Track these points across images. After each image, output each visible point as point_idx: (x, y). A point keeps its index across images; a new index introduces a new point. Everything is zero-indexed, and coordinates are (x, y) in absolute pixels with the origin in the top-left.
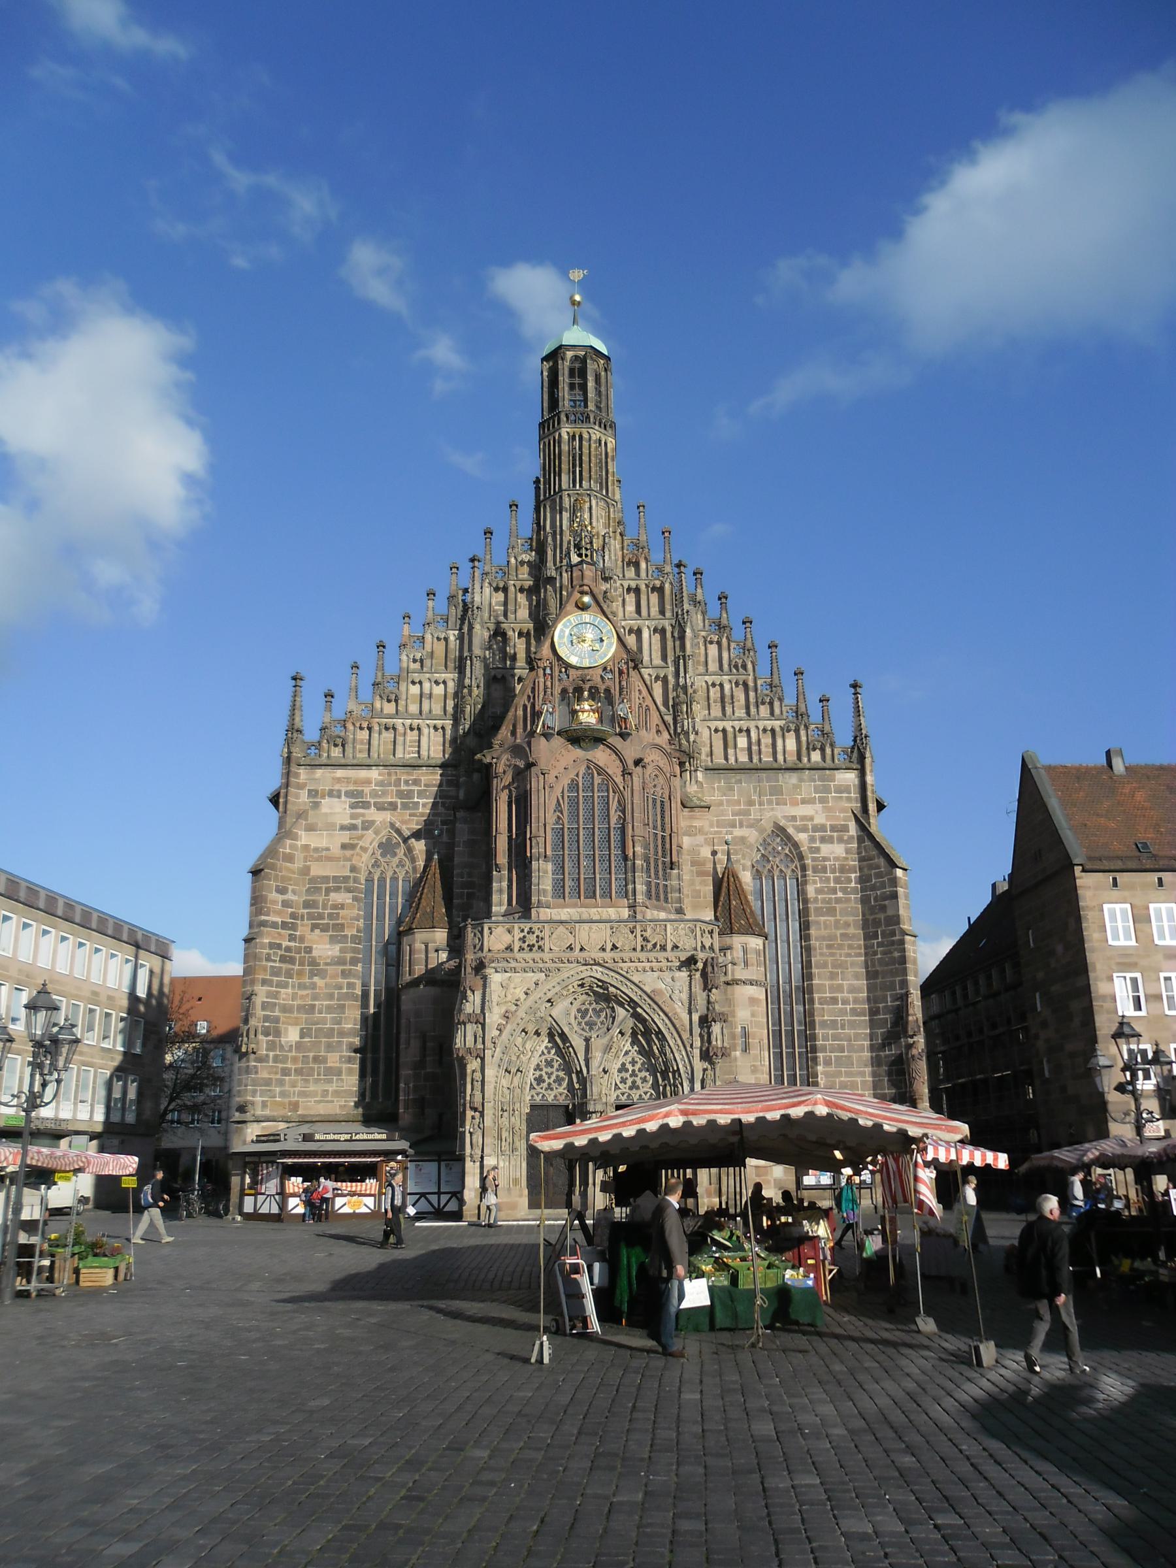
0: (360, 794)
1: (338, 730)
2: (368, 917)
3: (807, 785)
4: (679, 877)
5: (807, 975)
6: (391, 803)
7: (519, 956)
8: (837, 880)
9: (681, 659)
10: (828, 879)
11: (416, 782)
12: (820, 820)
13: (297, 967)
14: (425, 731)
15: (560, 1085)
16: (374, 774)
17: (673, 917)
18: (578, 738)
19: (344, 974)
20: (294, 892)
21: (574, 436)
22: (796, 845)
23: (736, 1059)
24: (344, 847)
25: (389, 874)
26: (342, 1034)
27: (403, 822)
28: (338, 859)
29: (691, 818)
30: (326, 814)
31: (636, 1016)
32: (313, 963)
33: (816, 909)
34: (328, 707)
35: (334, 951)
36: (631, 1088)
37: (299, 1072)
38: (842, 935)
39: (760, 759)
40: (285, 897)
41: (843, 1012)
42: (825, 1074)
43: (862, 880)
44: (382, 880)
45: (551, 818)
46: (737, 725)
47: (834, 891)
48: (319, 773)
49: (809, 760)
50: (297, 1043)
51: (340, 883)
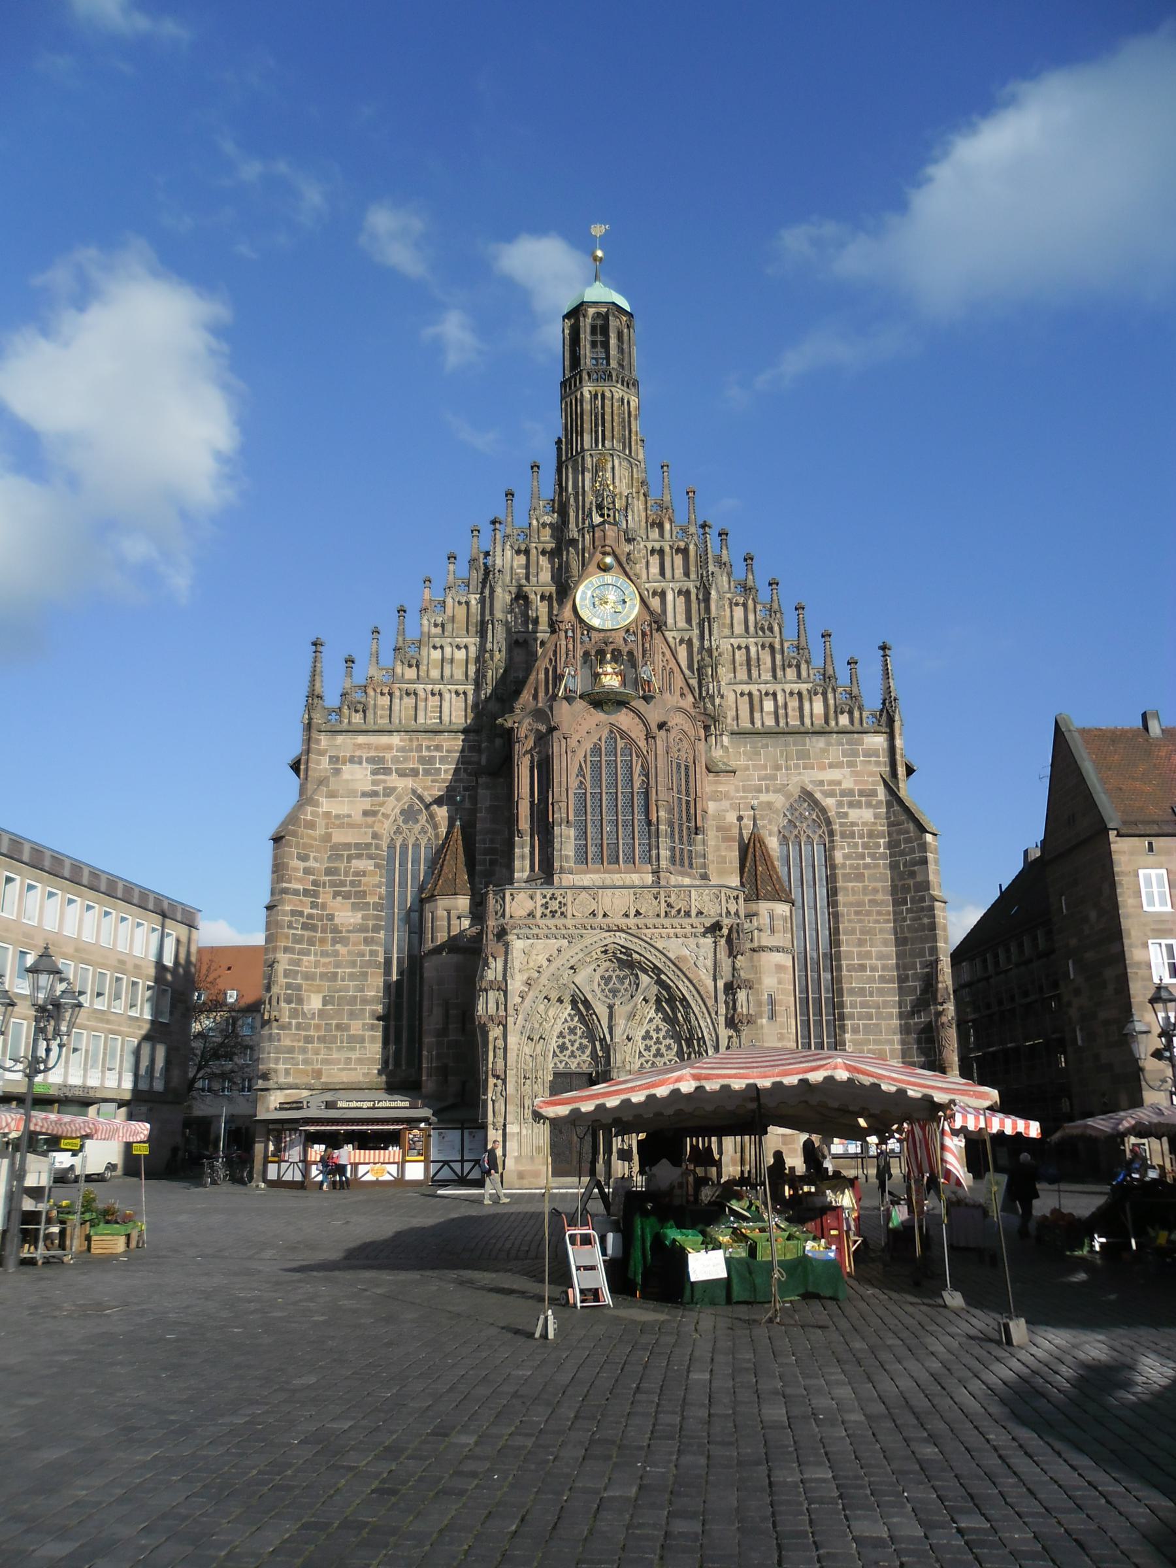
0: (382, 760)
1: (358, 696)
2: (390, 884)
3: (835, 749)
4: (704, 842)
5: (834, 942)
6: (412, 769)
7: (541, 922)
8: (865, 846)
9: (706, 622)
10: (856, 845)
11: (438, 748)
12: (848, 784)
13: (319, 935)
14: (447, 696)
15: (583, 1052)
16: (396, 740)
17: (698, 882)
18: (600, 701)
19: (367, 941)
20: (316, 859)
21: (596, 395)
22: (823, 810)
23: (762, 1026)
24: (366, 813)
25: (411, 842)
26: (364, 1001)
27: (424, 789)
28: (359, 826)
29: (716, 782)
30: (347, 781)
31: (660, 983)
32: (336, 930)
33: (844, 875)
34: (349, 674)
35: (356, 918)
36: (655, 1056)
37: (322, 1039)
38: (870, 901)
39: (787, 723)
40: (307, 864)
41: (871, 980)
42: (854, 1042)
43: (890, 845)
44: (404, 847)
45: (574, 783)
46: (763, 688)
47: (863, 857)
48: (340, 739)
49: (837, 723)
50: (320, 1010)
51: (361, 851)
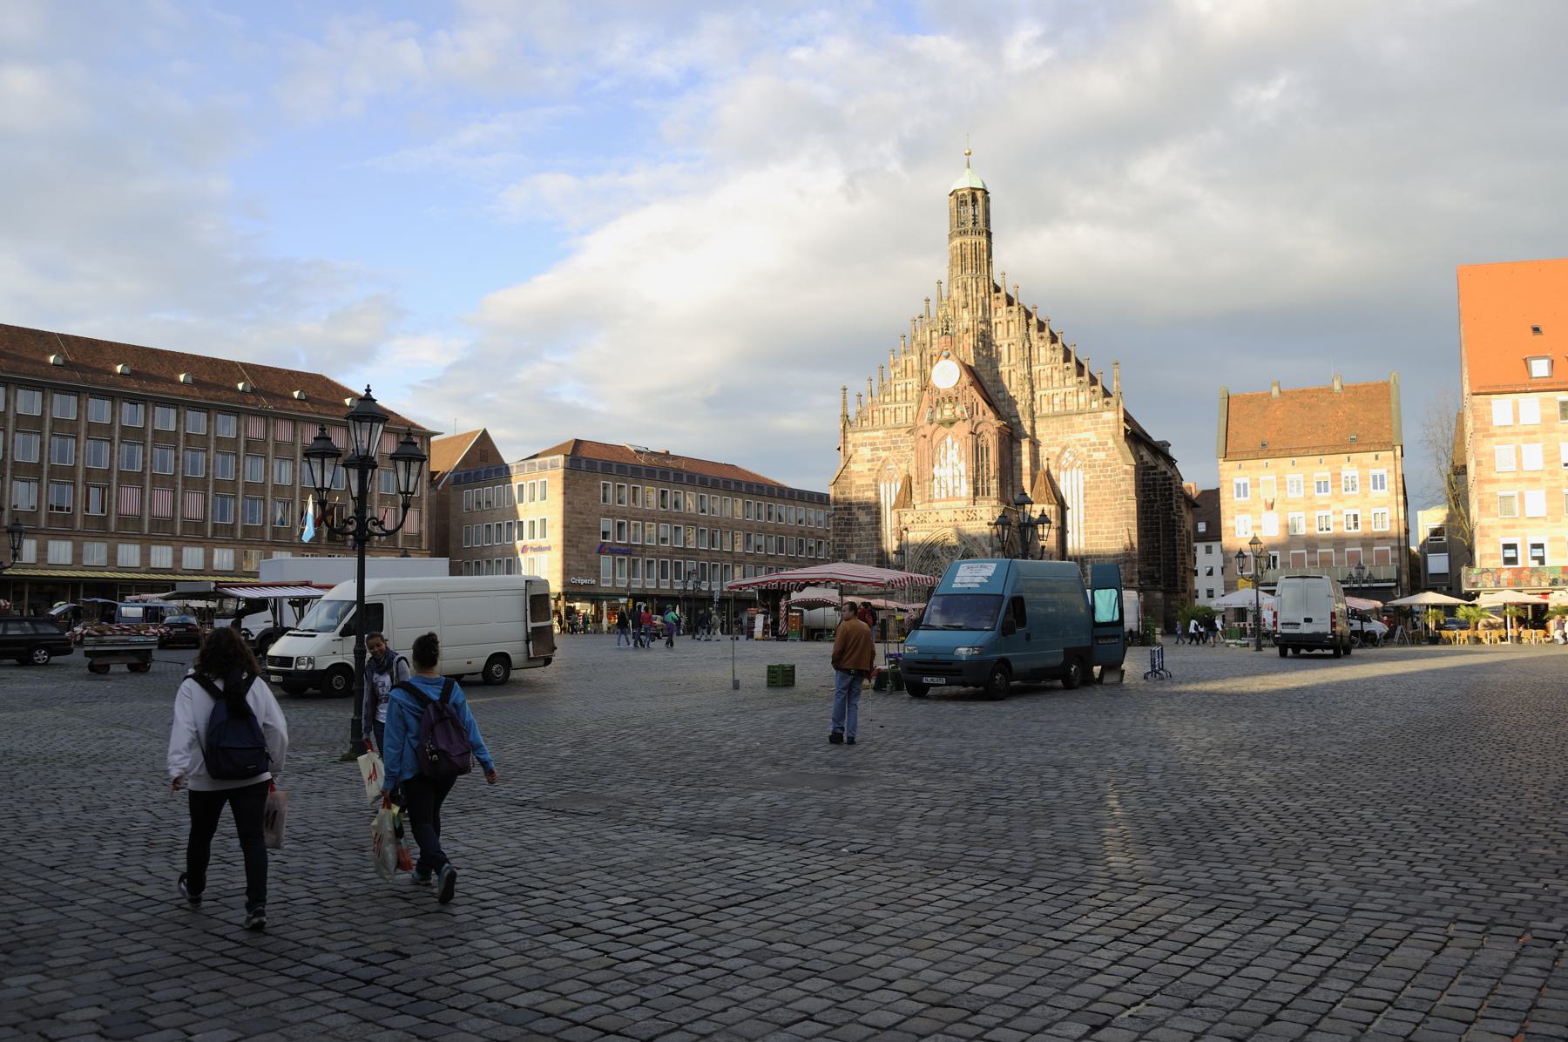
16: (880, 434)
35: (868, 519)
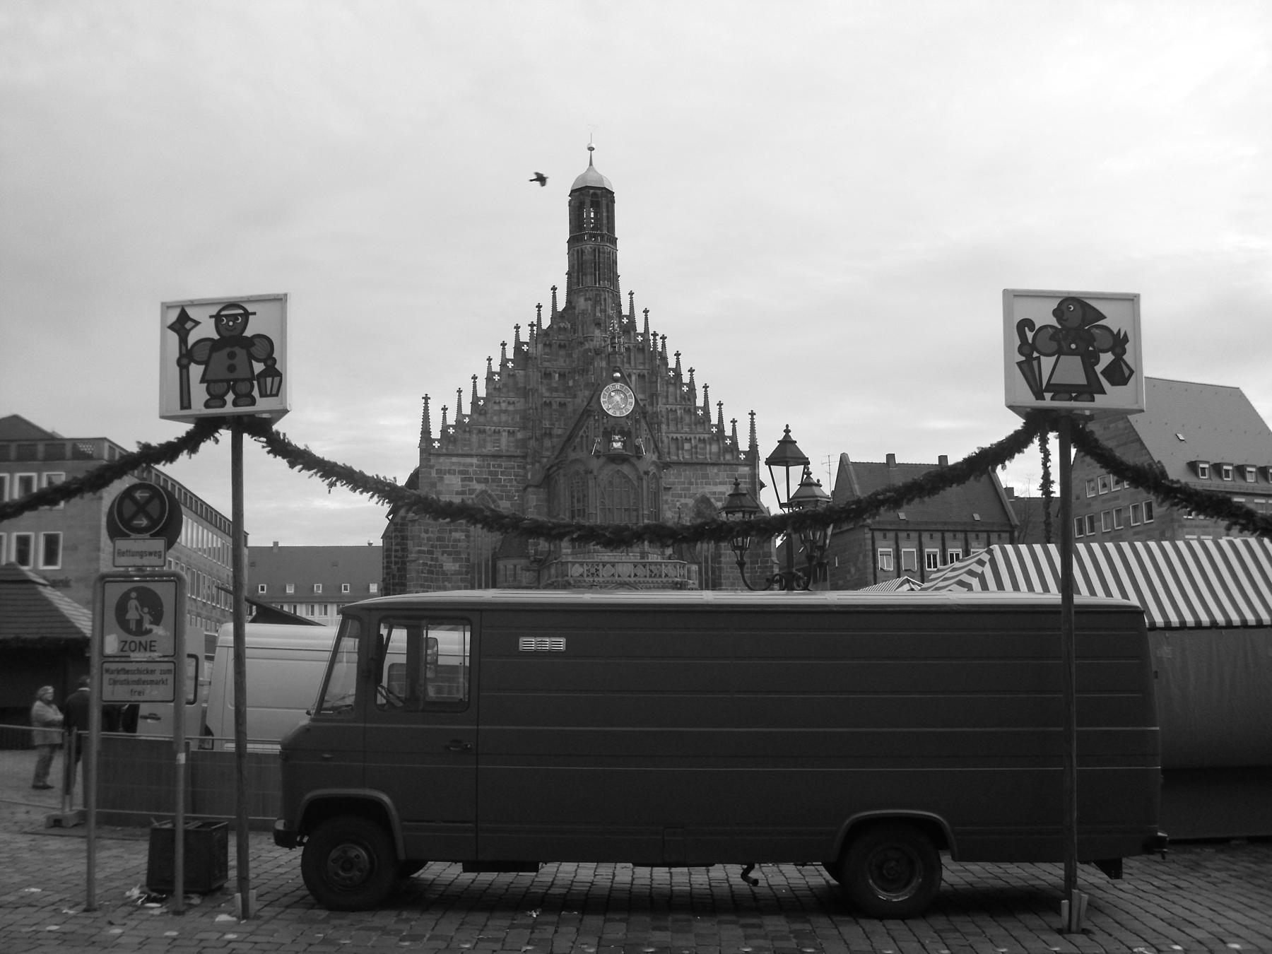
11: (500, 466)
16: (474, 461)
32: (444, 573)
35: (456, 567)
48: (442, 459)
